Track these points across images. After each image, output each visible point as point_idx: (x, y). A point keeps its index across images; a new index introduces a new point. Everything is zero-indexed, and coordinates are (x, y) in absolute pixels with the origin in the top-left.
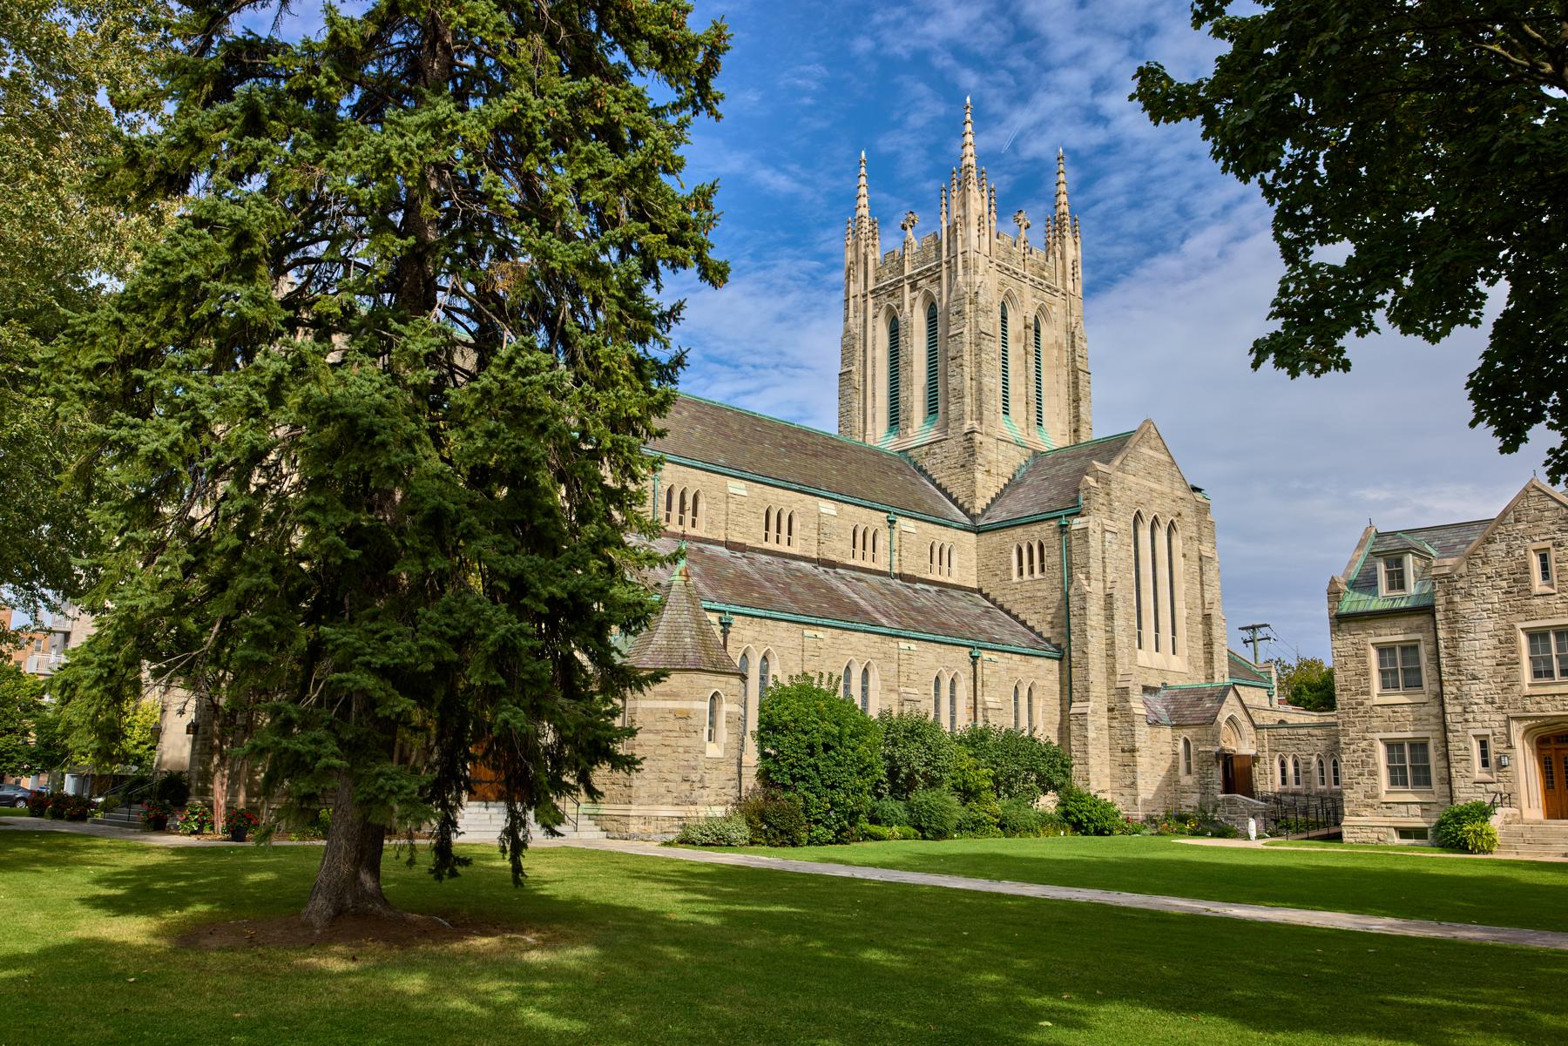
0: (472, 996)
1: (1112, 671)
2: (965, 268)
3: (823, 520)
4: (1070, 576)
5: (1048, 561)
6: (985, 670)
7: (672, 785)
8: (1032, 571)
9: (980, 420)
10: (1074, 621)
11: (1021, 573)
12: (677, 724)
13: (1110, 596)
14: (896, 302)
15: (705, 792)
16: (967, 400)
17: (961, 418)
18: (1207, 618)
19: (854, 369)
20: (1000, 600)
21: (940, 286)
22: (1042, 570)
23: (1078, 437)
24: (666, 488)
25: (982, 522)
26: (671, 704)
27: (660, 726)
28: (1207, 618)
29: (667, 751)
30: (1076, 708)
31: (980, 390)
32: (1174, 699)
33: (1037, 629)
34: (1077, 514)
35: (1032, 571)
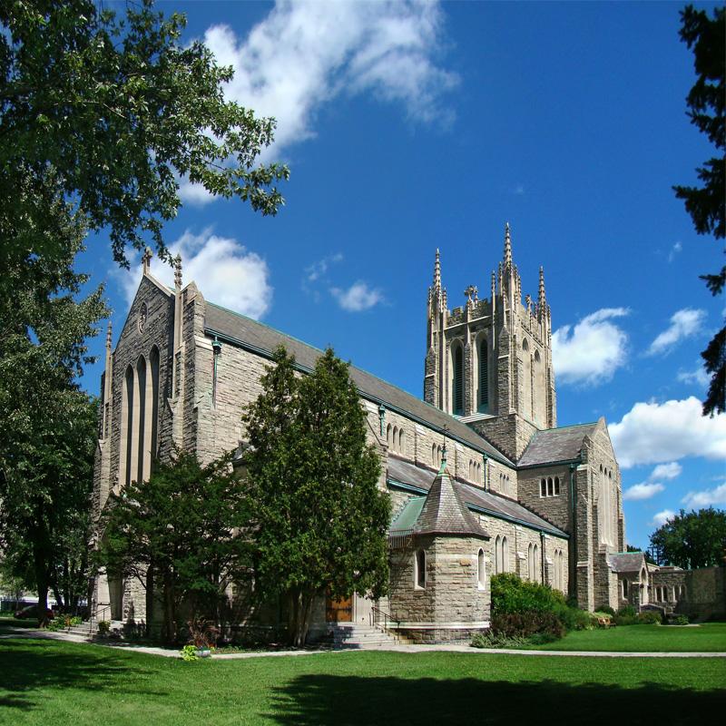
0: (311, 690)
1: (596, 545)
2: (508, 320)
3: (458, 454)
4: (575, 495)
5: (561, 488)
6: (547, 543)
7: (460, 609)
8: (551, 493)
9: (517, 408)
10: (579, 519)
11: (544, 493)
12: (460, 570)
13: (596, 507)
14: (461, 337)
15: (478, 613)
16: (510, 396)
17: (506, 408)
18: (620, 521)
19: (509, 356)
20: (532, 507)
21: (491, 330)
22: (557, 492)
23: (551, 425)
24: (387, 425)
25: (519, 465)
26: (457, 557)
27: (452, 570)
28: (620, 521)
29: (456, 587)
30: (579, 564)
31: (516, 391)
32: (615, 559)
33: (555, 523)
34: (580, 463)
35: (551, 493)
